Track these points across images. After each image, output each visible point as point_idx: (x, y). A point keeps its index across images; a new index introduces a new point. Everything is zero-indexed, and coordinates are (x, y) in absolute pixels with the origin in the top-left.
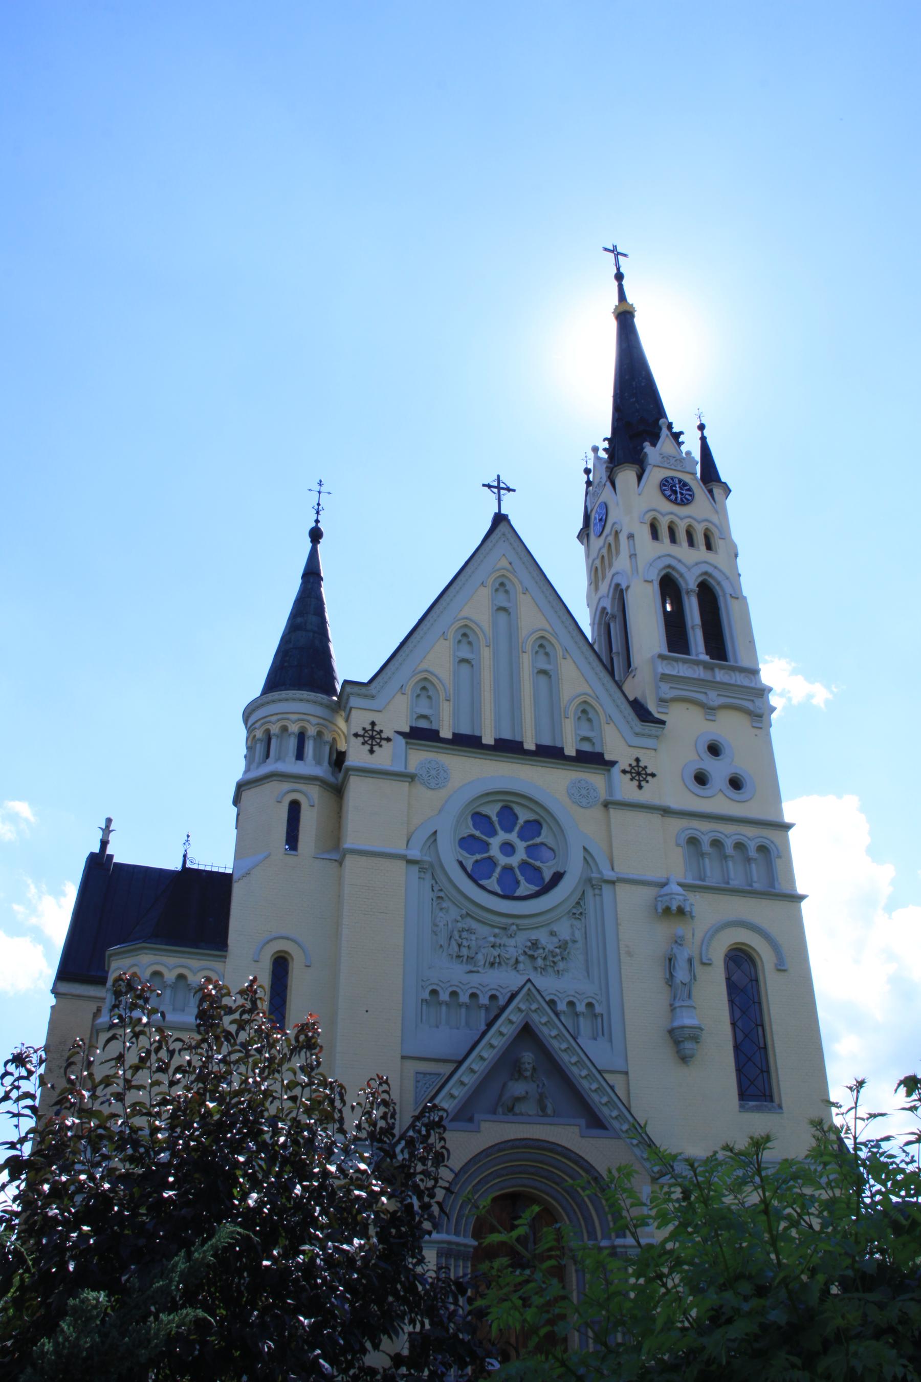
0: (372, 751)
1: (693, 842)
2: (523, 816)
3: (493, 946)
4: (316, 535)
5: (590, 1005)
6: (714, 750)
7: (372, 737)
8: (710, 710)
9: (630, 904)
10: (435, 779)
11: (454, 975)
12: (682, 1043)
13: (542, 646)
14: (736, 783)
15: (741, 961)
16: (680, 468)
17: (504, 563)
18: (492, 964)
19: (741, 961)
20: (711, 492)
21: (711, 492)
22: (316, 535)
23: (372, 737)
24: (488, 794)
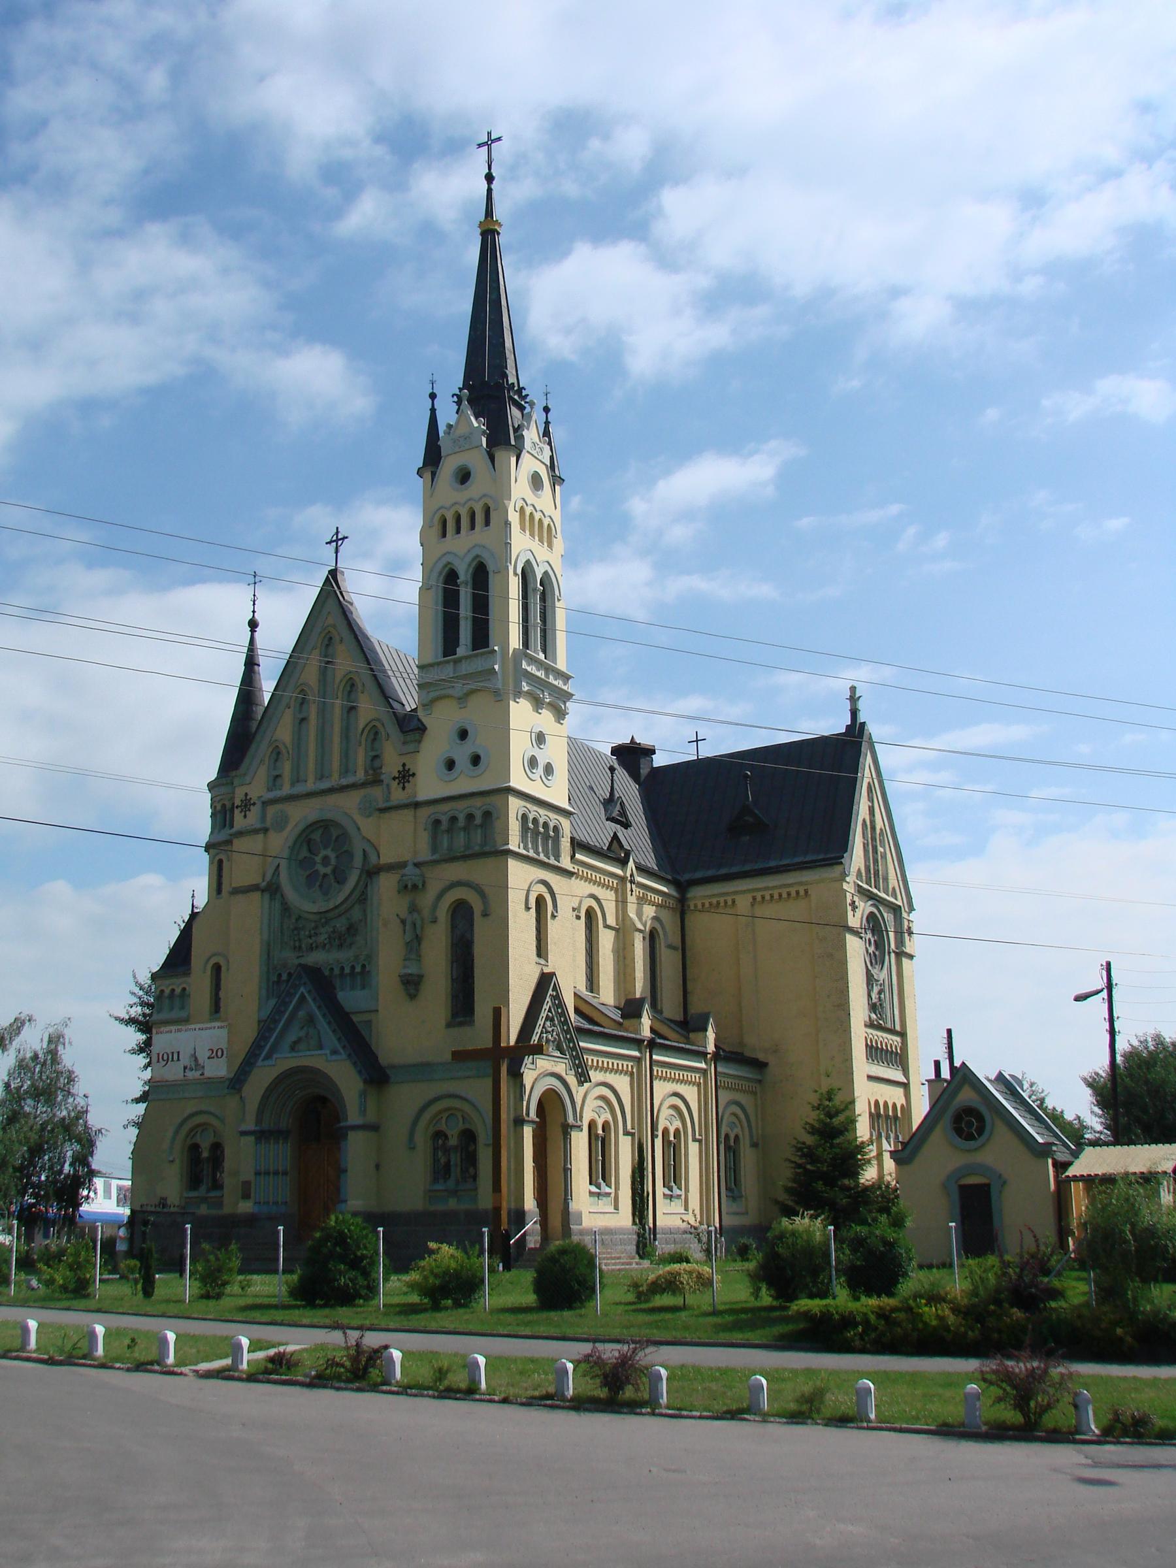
0: (245, 816)
1: (437, 822)
2: (335, 833)
3: (310, 937)
4: (253, 625)
5: (364, 966)
6: (463, 734)
7: (247, 804)
8: (463, 699)
9: (386, 884)
10: (281, 823)
11: (291, 958)
12: (412, 984)
13: (351, 686)
14: (476, 760)
15: (462, 914)
16: (467, 447)
17: (330, 621)
18: (312, 949)
19: (462, 914)
20: (492, 458)
21: (492, 458)
22: (253, 625)
23: (247, 804)
24: (311, 825)
